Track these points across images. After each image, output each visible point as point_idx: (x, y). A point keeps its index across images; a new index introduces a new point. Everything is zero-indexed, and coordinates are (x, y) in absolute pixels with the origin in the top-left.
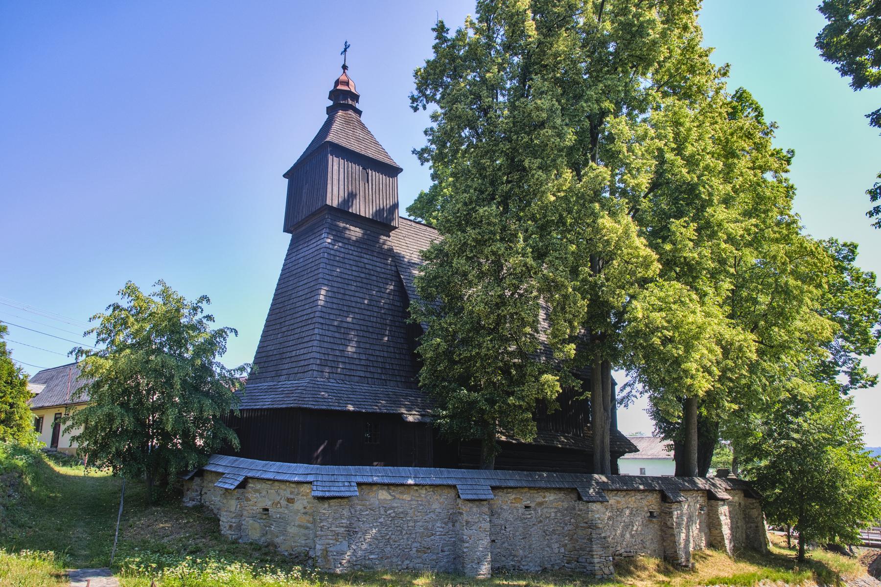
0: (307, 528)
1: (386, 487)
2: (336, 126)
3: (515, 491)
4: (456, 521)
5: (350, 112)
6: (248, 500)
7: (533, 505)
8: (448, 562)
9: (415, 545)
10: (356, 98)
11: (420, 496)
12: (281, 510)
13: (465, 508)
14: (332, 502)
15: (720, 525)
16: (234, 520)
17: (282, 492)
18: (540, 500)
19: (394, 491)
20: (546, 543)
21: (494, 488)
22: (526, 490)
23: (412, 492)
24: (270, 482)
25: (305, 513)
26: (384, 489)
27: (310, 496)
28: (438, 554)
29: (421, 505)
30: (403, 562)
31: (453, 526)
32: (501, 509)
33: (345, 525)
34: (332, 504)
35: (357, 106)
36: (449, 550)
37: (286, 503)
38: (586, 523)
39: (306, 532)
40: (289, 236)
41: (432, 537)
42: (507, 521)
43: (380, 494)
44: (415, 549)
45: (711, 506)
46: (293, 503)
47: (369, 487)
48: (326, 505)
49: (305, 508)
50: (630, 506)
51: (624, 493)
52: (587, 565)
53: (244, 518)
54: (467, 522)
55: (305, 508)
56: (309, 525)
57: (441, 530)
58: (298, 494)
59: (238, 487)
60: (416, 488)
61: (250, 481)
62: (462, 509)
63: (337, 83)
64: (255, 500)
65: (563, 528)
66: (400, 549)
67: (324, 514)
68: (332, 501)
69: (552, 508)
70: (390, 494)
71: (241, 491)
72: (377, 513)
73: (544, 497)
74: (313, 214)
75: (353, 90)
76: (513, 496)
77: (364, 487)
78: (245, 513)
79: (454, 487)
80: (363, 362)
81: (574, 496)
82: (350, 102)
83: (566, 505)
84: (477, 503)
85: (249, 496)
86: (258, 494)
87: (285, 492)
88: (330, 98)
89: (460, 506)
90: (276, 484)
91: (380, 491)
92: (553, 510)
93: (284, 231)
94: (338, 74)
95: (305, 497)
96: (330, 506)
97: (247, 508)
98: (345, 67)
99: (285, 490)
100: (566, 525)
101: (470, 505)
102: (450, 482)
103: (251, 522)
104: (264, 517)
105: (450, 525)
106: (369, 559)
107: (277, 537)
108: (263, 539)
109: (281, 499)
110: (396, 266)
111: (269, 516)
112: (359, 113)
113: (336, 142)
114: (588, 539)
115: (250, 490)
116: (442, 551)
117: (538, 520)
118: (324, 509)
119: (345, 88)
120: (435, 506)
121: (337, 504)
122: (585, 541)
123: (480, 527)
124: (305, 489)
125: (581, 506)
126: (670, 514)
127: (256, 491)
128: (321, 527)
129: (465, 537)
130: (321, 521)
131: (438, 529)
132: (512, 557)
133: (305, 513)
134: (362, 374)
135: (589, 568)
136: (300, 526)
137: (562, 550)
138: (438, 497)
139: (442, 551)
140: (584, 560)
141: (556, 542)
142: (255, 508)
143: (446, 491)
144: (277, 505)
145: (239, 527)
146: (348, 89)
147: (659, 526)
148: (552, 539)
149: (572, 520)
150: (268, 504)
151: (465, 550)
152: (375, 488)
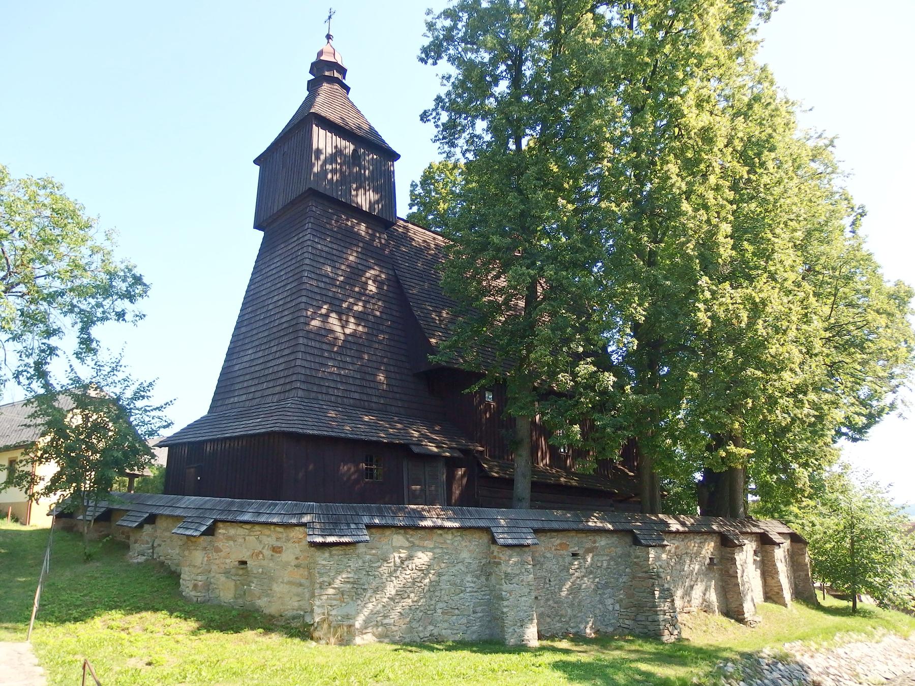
0: (301, 585)
1: (402, 531)
2: (319, 100)
3: (560, 535)
4: (490, 574)
5: (337, 86)
6: (218, 550)
7: (581, 552)
8: (481, 626)
9: (440, 605)
10: (343, 71)
11: (445, 542)
12: (265, 563)
13: (504, 555)
14: (335, 550)
15: (777, 573)
16: (200, 578)
17: (266, 540)
18: (589, 545)
19: (412, 535)
20: (597, 599)
21: (536, 531)
22: (573, 534)
23: (435, 538)
24: (248, 527)
25: (297, 566)
26: (399, 533)
27: (304, 543)
28: (469, 616)
29: (446, 553)
30: (425, 628)
31: (487, 580)
32: (545, 557)
33: (351, 580)
34: (334, 552)
35: (346, 82)
36: (483, 611)
37: (271, 553)
38: (646, 572)
39: (300, 589)
40: (261, 234)
41: (462, 595)
42: (551, 572)
43: (394, 540)
44: (439, 611)
45: (766, 552)
46: (280, 552)
47: (380, 531)
48: (327, 555)
49: (297, 558)
50: (689, 551)
51: (683, 536)
52: (648, 623)
53: (212, 574)
54: (507, 575)
55: (297, 558)
56: (303, 581)
57: (472, 585)
58: (288, 540)
59: (204, 534)
60: (439, 532)
61: (220, 525)
62: (500, 558)
63: (320, 53)
64: (228, 550)
65: (617, 580)
66: (421, 611)
67: (324, 566)
68: (334, 548)
69: (604, 555)
70: (407, 540)
71: (209, 538)
72: (392, 564)
73: (595, 542)
74: (293, 203)
75: (340, 63)
76: (558, 542)
77: (373, 530)
78: (214, 567)
79: (487, 530)
80: (358, 382)
81: (628, 540)
82: (336, 75)
83: (619, 551)
84: (518, 549)
85: (220, 545)
86: (231, 543)
87: (269, 539)
88: (311, 72)
89: (495, 554)
90: (257, 528)
91: (395, 536)
92: (605, 558)
93: (255, 227)
94: (322, 44)
95: (297, 545)
96: (331, 555)
97: (217, 562)
98: (329, 37)
99: (268, 536)
100: (621, 575)
101: (508, 552)
102: (482, 524)
103: (223, 578)
104: (241, 572)
105: (483, 579)
106: (382, 625)
107: (259, 598)
108: (240, 601)
109: (263, 548)
110: (394, 270)
111: (247, 571)
112: (347, 89)
113: (323, 114)
114: (648, 593)
115: (221, 537)
116: (474, 612)
117: (588, 571)
118: (323, 559)
119: (331, 59)
120: (465, 555)
121: (341, 552)
122: (645, 594)
123: (522, 581)
124: (298, 532)
125: (638, 551)
126: (733, 561)
127: (230, 538)
128: (321, 583)
129: (504, 593)
130: (321, 575)
131: (467, 584)
132: (558, 618)
133: (297, 566)
134: (357, 396)
135: (651, 628)
136: (290, 583)
137: (617, 607)
138: (468, 544)
139: (474, 612)
140: (643, 618)
141: (610, 597)
142: (228, 561)
143: (477, 535)
144: (257, 555)
145: (208, 586)
146: (333, 60)
147: (720, 575)
148: (604, 594)
149: (627, 570)
150: (244, 555)
151: (505, 610)
152: (388, 532)
